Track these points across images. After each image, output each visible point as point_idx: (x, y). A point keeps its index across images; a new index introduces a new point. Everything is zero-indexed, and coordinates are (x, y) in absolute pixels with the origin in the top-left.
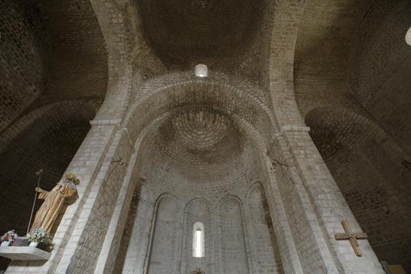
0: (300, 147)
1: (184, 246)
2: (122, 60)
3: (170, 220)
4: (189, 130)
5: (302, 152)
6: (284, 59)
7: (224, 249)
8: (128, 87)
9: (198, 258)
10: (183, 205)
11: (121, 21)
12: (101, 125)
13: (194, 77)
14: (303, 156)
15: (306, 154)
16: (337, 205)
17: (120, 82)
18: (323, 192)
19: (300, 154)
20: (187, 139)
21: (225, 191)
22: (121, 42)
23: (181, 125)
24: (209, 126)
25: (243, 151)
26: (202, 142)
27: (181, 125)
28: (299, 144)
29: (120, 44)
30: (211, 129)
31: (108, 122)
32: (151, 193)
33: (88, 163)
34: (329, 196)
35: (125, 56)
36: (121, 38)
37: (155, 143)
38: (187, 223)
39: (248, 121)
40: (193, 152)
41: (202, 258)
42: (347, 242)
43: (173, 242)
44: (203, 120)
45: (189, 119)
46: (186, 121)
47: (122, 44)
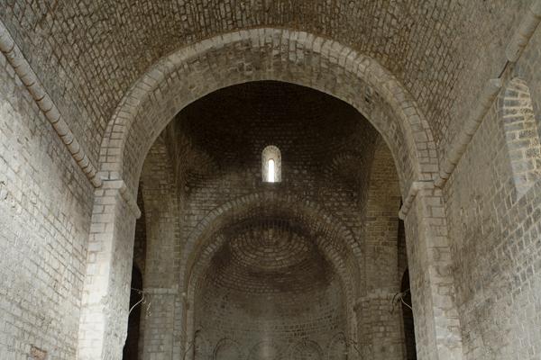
0: (382, 322)
2: (162, 192)
5: (382, 329)
6: (389, 191)
11: (162, 152)
13: (262, 185)
15: (385, 332)
17: (162, 221)
19: (379, 332)
20: (249, 259)
21: (303, 334)
22: (161, 170)
24: (283, 243)
25: (329, 284)
26: (271, 262)
28: (382, 318)
29: (159, 173)
30: (284, 248)
32: (207, 344)
35: (167, 187)
36: (161, 167)
40: (256, 275)
45: (252, 237)
46: (249, 240)
47: (163, 173)
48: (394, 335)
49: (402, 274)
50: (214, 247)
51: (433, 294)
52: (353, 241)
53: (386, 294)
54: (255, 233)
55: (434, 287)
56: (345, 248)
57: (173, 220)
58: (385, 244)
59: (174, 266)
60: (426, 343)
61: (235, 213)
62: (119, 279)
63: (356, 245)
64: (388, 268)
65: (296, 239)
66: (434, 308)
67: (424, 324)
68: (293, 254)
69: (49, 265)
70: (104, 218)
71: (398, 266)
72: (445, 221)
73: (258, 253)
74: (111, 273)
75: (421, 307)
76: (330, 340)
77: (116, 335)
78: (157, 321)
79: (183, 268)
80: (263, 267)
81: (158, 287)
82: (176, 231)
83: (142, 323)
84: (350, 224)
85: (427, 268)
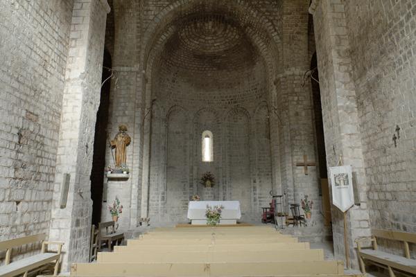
0: (296, 93)
1: (195, 154)
3: (180, 130)
4: (196, 36)
7: (231, 156)
8: (135, 21)
9: (208, 163)
14: (295, 103)
16: (306, 143)
18: (300, 134)
19: (293, 100)
20: (194, 44)
21: (235, 102)
25: (255, 64)
26: (210, 47)
28: (296, 90)
30: (221, 36)
34: (303, 138)
38: (196, 133)
40: (201, 57)
41: (211, 162)
42: (302, 167)
45: (196, 28)
46: (194, 30)
48: (305, 103)
49: (311, 56)
50: (167, 35)
51: (335, 71)
52: (273, 30)
53: (299, 71)
54: (198, 24)
55: (336, 66)
56: (267, 36)
57: (135, 14)
58: (298, 33)
59: (136, 50)
60: (330, 109)
61: (183, 9)
62: (94, 60)
63: (276, 33)
64: (300, 52)
65: (230, 29)
66: (336, 82)
67: (328, 95)
68: (227, 40)
69: (40, 49)
70: (82, 13)
71: (309, 50)
72: (344, 15)
74: (88, 55)
75: (326, 81)
76: (256, 107)
77: (91, 103)
78: (123, 92)
79: (143, 52)
80: (205, 51)
81: (123, 66)
82: (137, 23)
83: (111, 94)
84: (271, 18)
85: (331, 52)
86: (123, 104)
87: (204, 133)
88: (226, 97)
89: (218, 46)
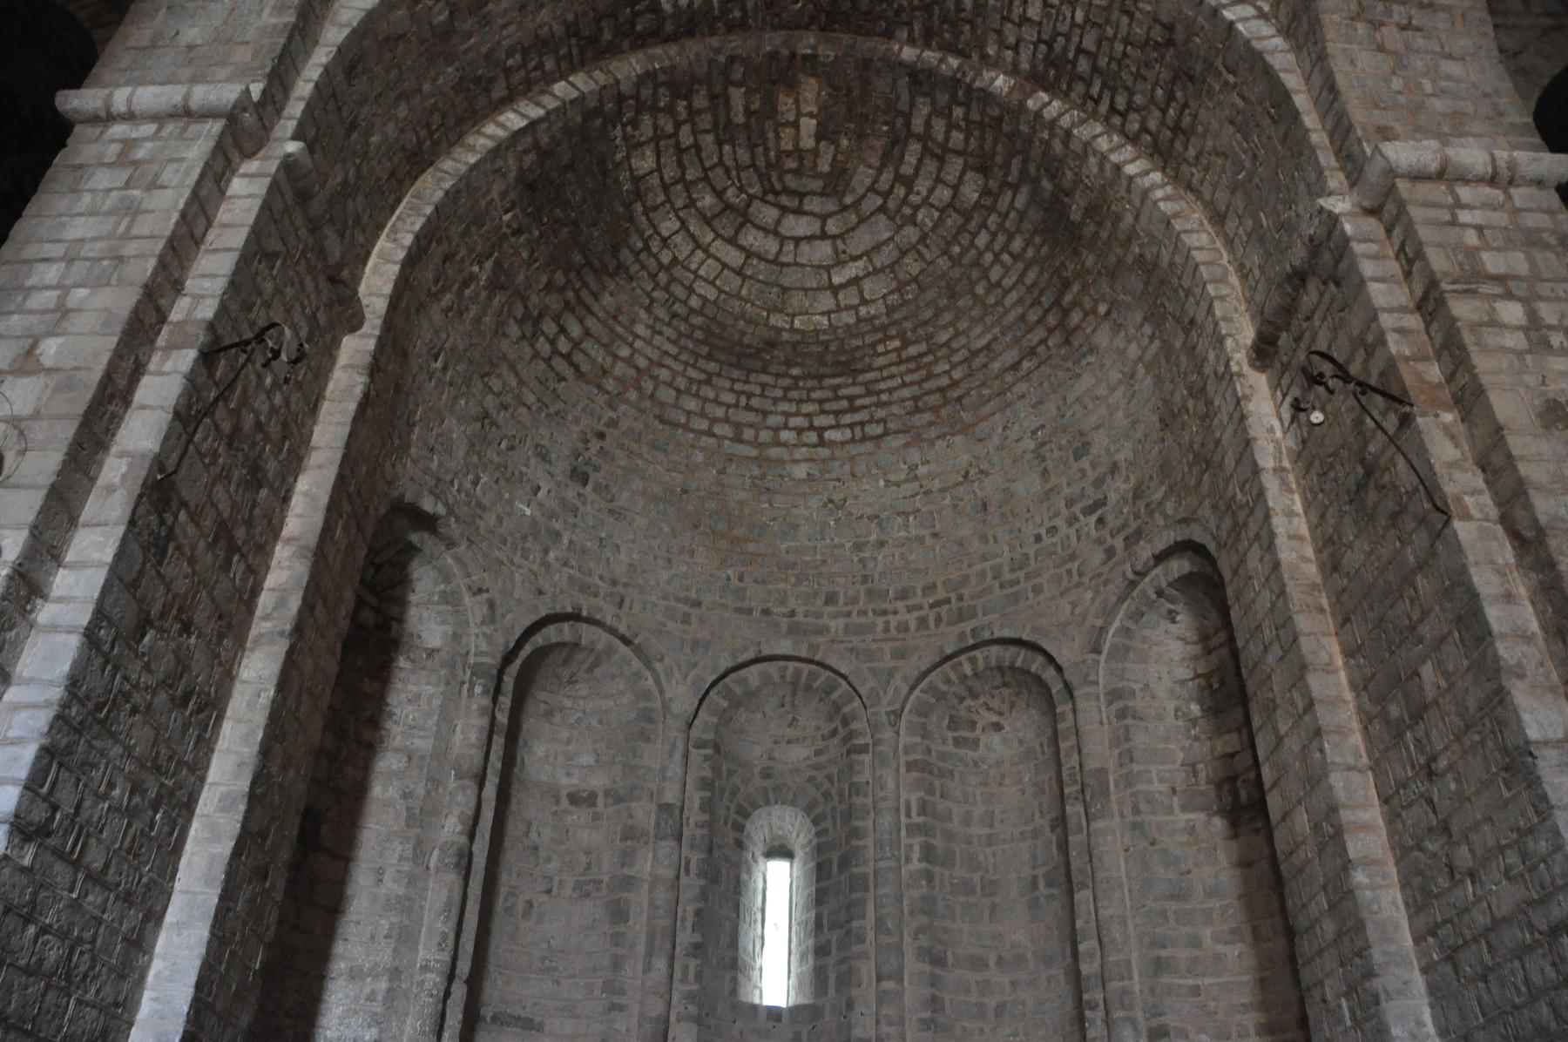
0: (1500, 279)
3: (598, 782)
5: (1512, 312)
7: (938, 961)
9: (774, 1014)
10: (682, 697)
12: (130, 117)
14: (1516, 340)
15: (1534, 324)
19: (1494, 323)
21: (961, 617)
23: (670, 173)
24: (862, 177)
27: (670, 173)
28: (1492, 262)
31: (173, 95)
32: (474, 608)
33: (50, 349)
37: (494, 286)
38: (707, 806)
39: (1134, 140)
41: (795, 1011)
43: (619, 913)
44: (820, 136)
73: (751, 238)
80: (777, 320)
86: (47, 299)
87: (760, 828)
88: (904, 595)
89: (855, 281)
